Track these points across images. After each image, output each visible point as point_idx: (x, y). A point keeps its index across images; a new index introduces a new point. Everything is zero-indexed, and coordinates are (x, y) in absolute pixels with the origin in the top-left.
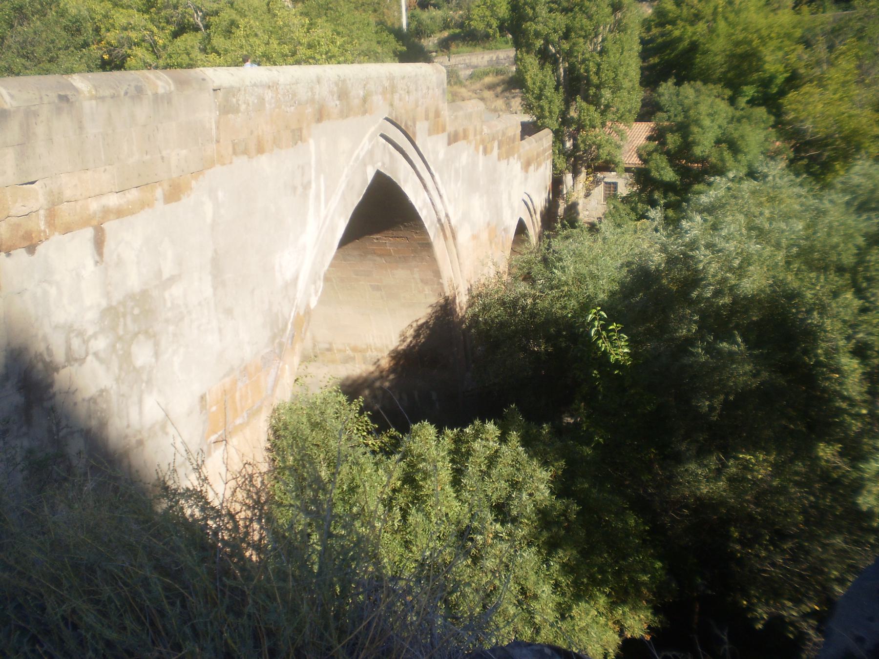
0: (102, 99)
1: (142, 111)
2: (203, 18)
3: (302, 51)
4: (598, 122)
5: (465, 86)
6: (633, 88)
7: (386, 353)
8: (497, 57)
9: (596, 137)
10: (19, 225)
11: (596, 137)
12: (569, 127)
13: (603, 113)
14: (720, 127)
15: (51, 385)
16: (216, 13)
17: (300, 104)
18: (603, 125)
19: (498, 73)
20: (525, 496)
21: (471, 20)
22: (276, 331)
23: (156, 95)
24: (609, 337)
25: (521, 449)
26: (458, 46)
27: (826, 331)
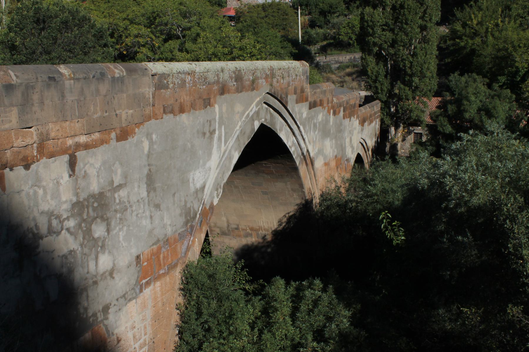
0: (78, 79)
1: (104, 88)
2: (182, 32)
3: (236, 52)
4: (410, 97)
5: (335, 74)
6: (432, 77)
7: (270, 231)
8: (354, 57)
9: (409, 106)
10: (20, 152)
11: (409, 106)
12: (393, 99)
13: (414, 91)
14: (481, 101)
15: (38, 247)
16: (189, 29)
17: (209, 84)
18: (414, 98)
19: (354, 66)
20: (333, 326)
21: (340, 35)
22: (189, 218)
23: (113, 78)
24: (393, 230)
25: (334, 296)
26: (331, 50)
27: (514, 233)
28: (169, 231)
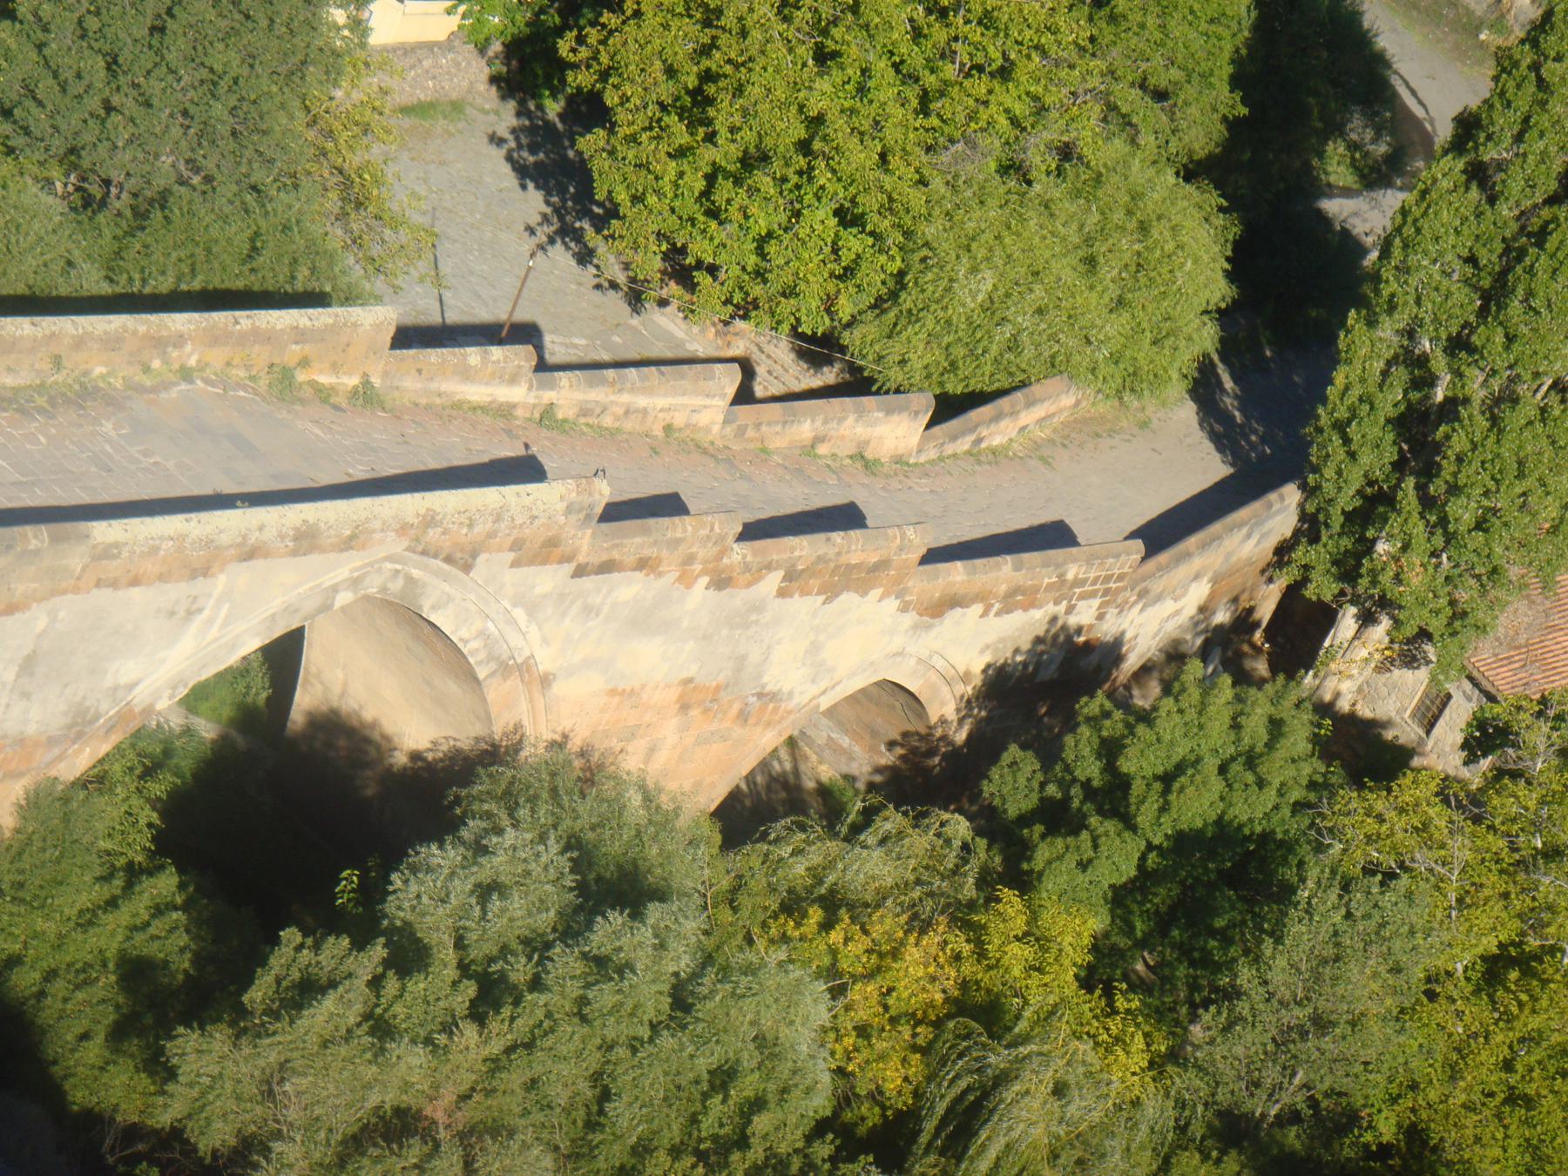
28: (31, 729)
